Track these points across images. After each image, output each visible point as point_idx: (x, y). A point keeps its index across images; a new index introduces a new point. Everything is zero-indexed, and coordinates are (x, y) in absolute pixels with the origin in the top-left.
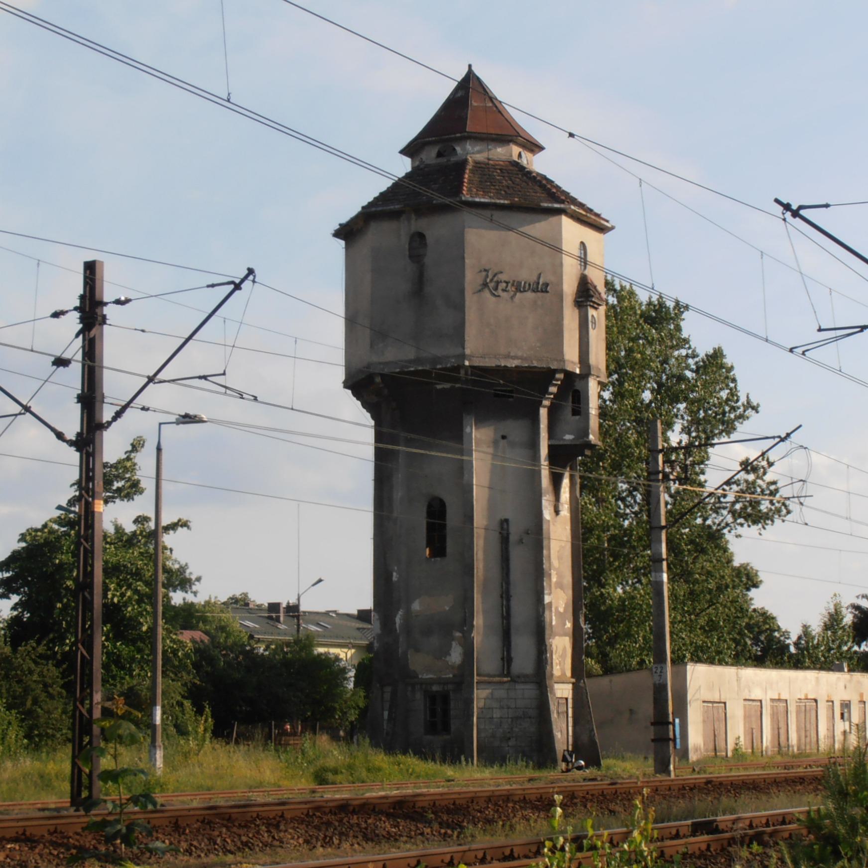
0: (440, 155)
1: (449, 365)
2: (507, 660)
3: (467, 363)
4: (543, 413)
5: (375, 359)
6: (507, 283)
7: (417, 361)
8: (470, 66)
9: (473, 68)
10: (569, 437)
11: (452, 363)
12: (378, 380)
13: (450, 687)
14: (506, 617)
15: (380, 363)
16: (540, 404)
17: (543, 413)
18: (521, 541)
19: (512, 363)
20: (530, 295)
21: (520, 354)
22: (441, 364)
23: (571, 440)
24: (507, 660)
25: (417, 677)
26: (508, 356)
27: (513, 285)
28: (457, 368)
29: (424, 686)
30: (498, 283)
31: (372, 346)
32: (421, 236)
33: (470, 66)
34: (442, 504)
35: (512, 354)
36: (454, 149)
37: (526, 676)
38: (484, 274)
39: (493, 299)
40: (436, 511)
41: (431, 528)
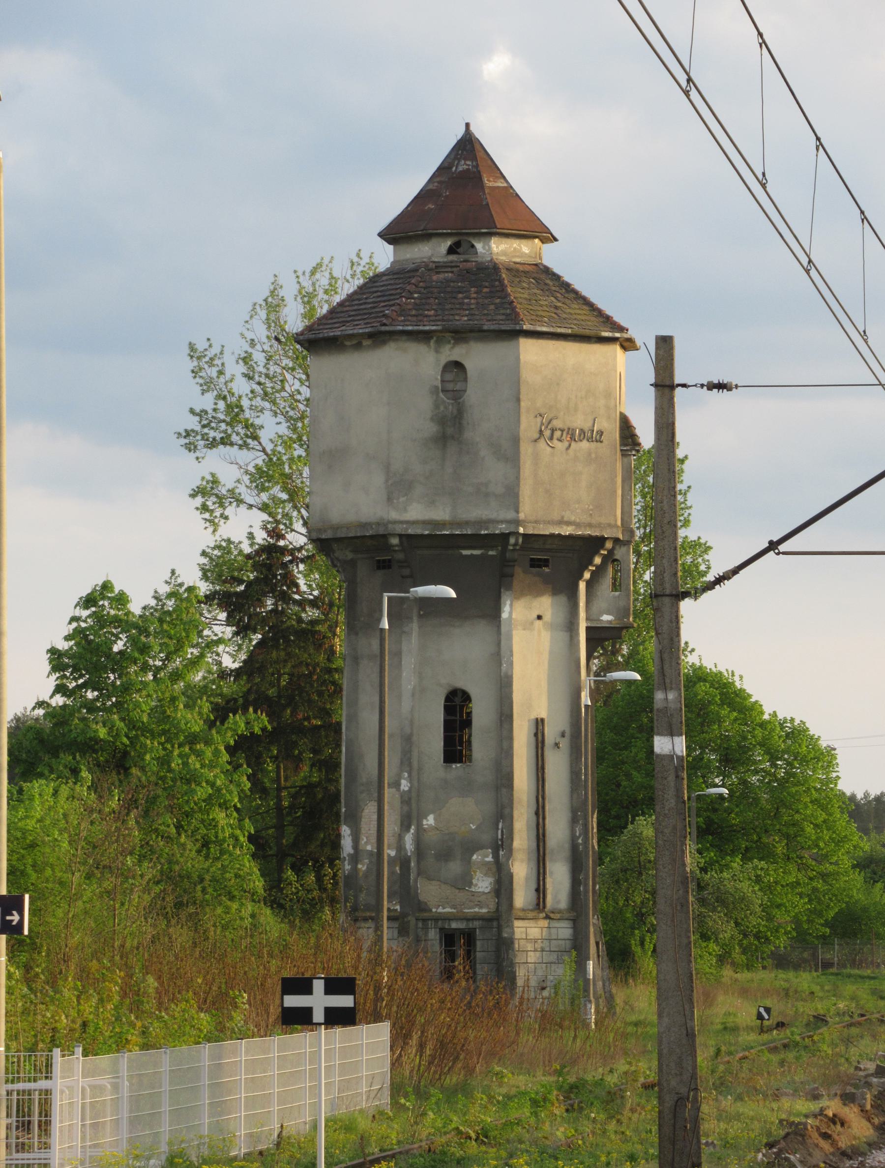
0: (451, 251)
1: (497, 532)
2: (540, 891)
3: (521, 530)
4: (582, 586)
5: (394, 515)
6: (562, 431)
7: (453, 524)
8: (467, 125)
9: (472, 128)
10: (606, 618)
11: (502, 528)
12: (395, 541)
13: (477, 924)
14: (540, 837)
15: (402, 522)
16: (581, 576)
17: (582, 586)
18: (557, 745)
19: (567, 531)
20: (585, 444)
21: (573, 518)
22: (487, 529)
23: (610, 622)
24: (540, 891)
25: (431, 910)
26: (561, 522)
27: (568, 433)
28: (505, 537)
29: (440, 922)
30: (553, 431)
31: (389, 500)
32: (458, 366)
33: (467, 125)
34: (466, 697)
35: (565, 519)
36: (473, 246)
37: (560, 912)
38: (539, 419)
39: (549, 449)
40: (457, 705)
41: (449, 726)
